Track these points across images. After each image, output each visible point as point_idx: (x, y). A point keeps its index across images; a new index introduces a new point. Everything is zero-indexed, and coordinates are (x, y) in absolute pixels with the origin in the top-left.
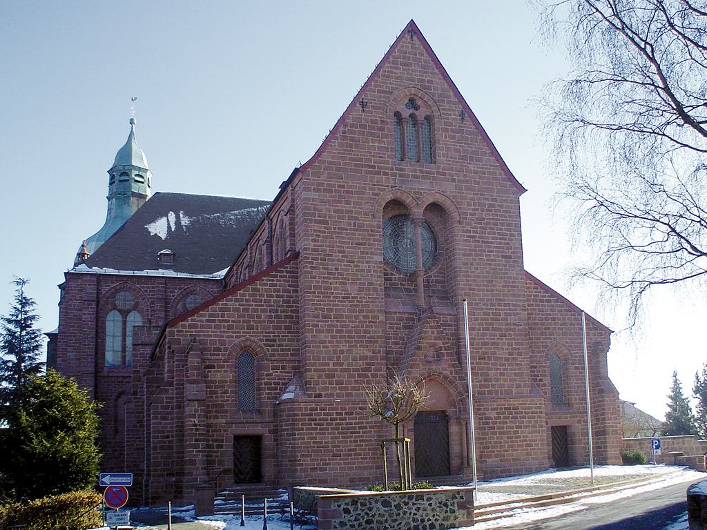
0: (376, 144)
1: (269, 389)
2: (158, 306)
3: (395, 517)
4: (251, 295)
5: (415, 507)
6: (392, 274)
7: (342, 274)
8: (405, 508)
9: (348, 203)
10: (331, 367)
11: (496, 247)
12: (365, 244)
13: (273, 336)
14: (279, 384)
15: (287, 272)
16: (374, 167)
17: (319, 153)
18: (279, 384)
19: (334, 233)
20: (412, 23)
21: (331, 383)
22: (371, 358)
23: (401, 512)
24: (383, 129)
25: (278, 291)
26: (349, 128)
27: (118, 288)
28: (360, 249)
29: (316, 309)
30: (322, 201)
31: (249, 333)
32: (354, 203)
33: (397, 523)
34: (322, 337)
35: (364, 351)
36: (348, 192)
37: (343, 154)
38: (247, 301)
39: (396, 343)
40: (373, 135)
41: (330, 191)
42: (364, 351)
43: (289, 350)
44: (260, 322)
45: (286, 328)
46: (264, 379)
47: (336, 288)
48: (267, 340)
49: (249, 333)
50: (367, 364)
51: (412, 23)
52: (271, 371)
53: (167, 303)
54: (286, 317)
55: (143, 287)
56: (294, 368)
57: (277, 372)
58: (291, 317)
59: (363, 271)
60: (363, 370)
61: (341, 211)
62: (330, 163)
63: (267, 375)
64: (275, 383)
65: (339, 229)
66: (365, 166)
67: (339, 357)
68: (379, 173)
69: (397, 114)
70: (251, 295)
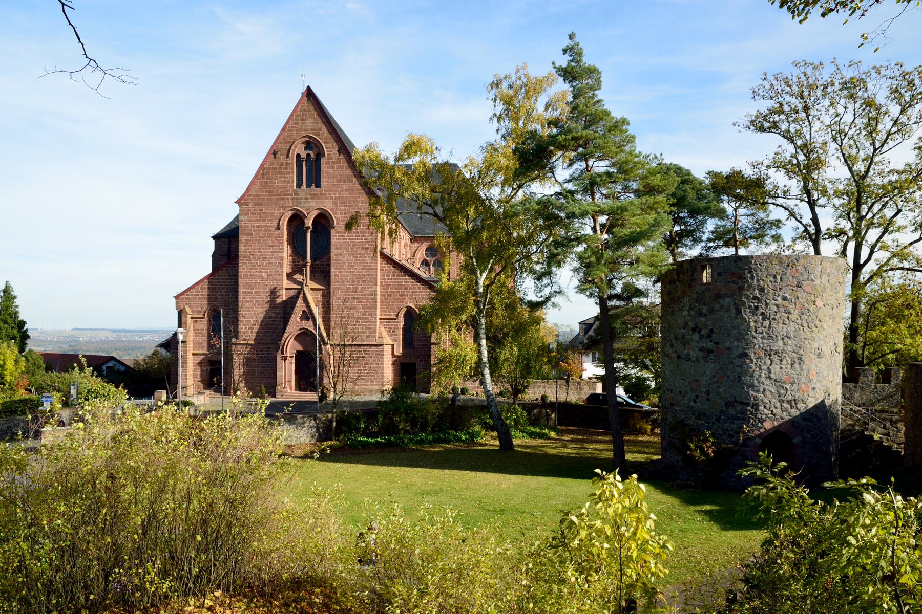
7: (259, 266)
9: (264, 220)
16: (280, 195)
17: (248, 189)
20: (309, 88)
22: (275, 317)
24: (286, 168)
25: (231, 276)
30: (250, 221)
36: (264, 213)
40: (280, 173)
41: (255, 214)
47: (256, 275)
51: (309, 88)
60: (270, 325)
61: (260, 226)
62: (254, 196)
68: (283, 199)
69: (298, 155)
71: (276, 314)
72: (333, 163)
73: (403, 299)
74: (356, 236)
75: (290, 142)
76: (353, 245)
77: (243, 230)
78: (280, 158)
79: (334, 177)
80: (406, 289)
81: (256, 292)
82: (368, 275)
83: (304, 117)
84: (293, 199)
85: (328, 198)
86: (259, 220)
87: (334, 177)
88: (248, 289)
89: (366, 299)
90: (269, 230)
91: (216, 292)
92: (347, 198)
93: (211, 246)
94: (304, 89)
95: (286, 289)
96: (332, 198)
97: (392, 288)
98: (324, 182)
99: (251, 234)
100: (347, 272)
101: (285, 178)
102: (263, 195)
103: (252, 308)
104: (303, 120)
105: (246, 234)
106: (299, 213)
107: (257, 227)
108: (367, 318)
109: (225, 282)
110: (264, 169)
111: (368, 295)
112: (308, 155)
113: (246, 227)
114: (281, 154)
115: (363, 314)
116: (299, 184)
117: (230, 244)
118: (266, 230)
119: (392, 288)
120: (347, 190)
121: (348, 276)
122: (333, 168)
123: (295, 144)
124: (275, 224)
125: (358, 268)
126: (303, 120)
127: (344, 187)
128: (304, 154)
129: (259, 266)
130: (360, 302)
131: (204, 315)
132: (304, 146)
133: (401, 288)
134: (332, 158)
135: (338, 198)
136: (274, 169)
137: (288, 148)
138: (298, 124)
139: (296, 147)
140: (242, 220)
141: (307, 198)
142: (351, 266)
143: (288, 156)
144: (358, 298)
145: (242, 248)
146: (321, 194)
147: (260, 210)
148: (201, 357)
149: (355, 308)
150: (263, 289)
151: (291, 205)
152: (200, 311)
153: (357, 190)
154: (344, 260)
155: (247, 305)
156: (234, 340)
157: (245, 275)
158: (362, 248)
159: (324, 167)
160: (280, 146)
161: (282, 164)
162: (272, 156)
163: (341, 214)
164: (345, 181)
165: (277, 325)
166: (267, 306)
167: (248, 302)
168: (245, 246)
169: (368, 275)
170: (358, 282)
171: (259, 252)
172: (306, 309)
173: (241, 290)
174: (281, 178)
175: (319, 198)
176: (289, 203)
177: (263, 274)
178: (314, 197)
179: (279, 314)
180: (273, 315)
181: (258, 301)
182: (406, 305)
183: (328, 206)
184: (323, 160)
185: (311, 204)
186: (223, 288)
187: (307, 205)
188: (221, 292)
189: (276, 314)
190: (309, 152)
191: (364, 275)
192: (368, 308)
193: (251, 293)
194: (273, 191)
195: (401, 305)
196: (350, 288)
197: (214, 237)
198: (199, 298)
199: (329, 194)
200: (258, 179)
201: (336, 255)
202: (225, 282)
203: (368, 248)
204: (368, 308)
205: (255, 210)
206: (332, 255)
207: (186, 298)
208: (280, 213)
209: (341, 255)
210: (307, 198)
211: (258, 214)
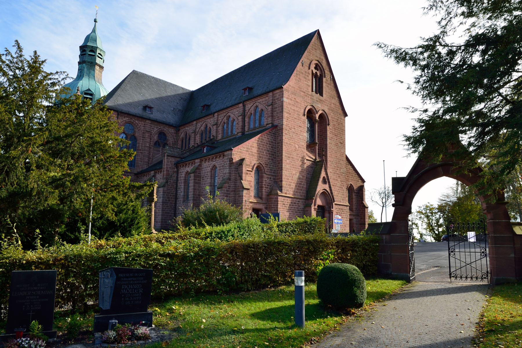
1: (266, 187)
2: (147, 135)
9: (297, 107)
19: (292, 119)
21: (290, 188)
22: (302, 179)
27: (127, 121)
47: (292, 145)
52: (266, 179)
53: (151, 135)
55: (139, 123)
56: (274, 179)
66: (302, 92)
71: (303, 176)
73: (349, 179)
75: (310, 60)
89: (342, 175)
95: (307, 160)
96: (328, 106)
98: (324, 95)
103: (290, 169)
105: (287, 113)
106: (313, 109)
108: (342, 188)
113: (287, 107)
128: (314, 71)
141: (317, 101)
149: (337, 180)
151: (310, 102)
159: (324, 84)
161: (306, 72)
172: (325, 176)
174: (305, 81)
180: (301, 177)
182: (350, 183)
184: (324, 79)
186: (265, 150)
188: (263, 152)
198: (249, 154)
205: (292, 97)
208: (305, 105)
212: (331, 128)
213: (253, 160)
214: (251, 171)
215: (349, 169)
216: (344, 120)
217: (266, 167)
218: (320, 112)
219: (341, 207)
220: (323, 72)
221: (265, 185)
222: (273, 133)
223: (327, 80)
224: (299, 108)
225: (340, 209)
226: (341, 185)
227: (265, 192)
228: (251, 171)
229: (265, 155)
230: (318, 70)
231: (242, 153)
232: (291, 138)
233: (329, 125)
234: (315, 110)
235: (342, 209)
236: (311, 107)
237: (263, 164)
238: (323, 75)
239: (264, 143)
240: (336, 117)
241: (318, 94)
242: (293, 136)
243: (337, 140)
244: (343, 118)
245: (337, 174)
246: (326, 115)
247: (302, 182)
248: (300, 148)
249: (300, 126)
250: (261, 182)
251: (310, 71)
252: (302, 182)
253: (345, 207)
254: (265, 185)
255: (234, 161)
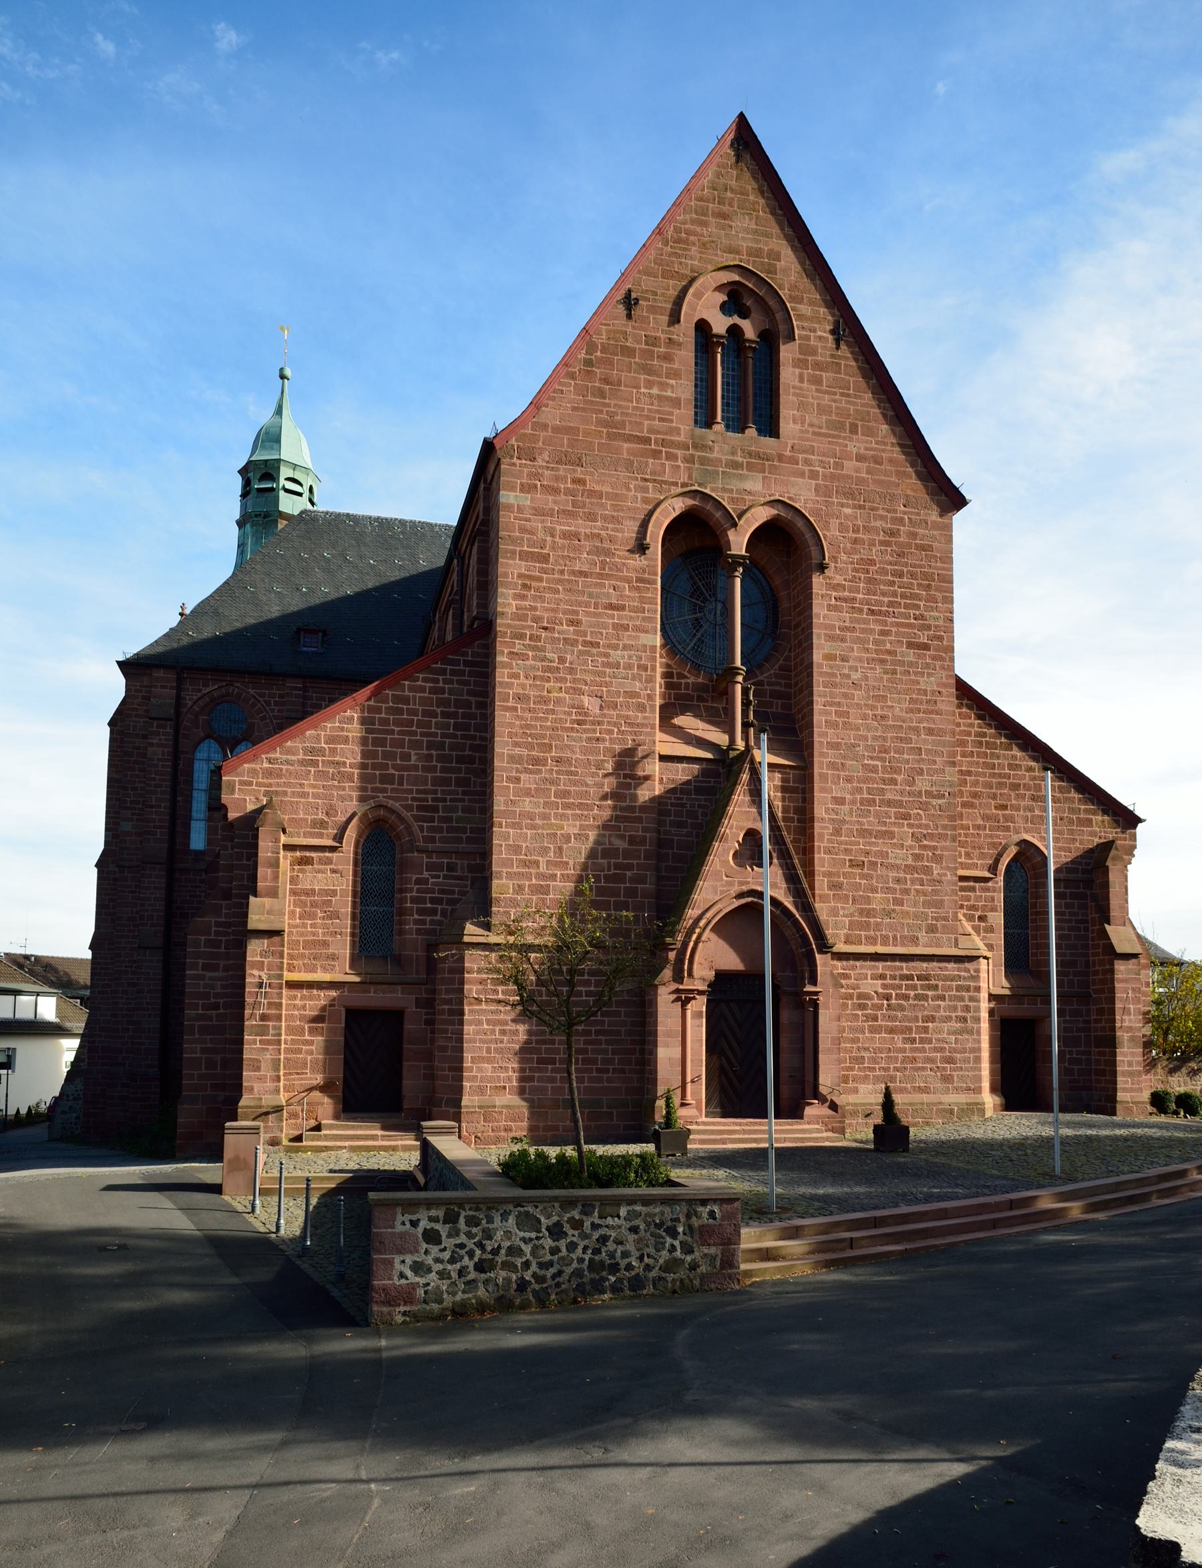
0: (655, 391)
1: (421, 912)
3: (548, 1257)
4: (391, 711)
5: (596, 1235)
6: (681, 676)
8: (572, 1234)
9: (591, 517)
10: (543, 868)
11: (898, 625)
12: (623, 608)
13: (434, 800)
14: (439, 901)
15: (466, 663)
16: (647, 441)
17: (536, 405)
18: (439, 901)
19: (560, 581)
20: (742, 122)
22: (627, 854)
23: (562, 1244)
24: (667, 358)
26: (599, 354)
28: (613, 617)
29: (516, 744)
31: (385, 790)
32: (605, 518)
33: (552, 1271)
34: (527, 804)
35: (613, 839)
36: (592, 493)
37: (583, 409)
38: (384, 722)
39: (680, 825)
40: (648, 370)
41: (556, 491)
42: (613, 839)
43: (464, 830)
44: (407, 768)
45: (459, 782)
46: (411, 890)
47: (558, 701)
48: (419, 808)
49: (385, 790)
50: (617, 866)
52: (426, 874)
54: (460, 760)
56: (471, 869)
57: (438, 877)
58: (471, 760)
59: (617, 666)
61: (576, 536)
62: (556, 430)
63: (418, 882)
64: (433, 901)
65: (573, 573)
66: (630, 438)
67: (560, 849)
68: (656, 454)
69: (702, 327)
70: (391, 711)
71: (632, 841)
72: (818, 366)
73: (1008, 819)
74: (891, 604)
76: (882, 633)
77: (513, 541)
78: (645, 320)
79: (822, 410)
80: (1015, 787)
81: (558, 761)
82: (930, 732)
83: (726, 208)
84: (689, 460)
85: (802, 475)
86: (571, 514)
87: (822, 410)
88: (531, 747)
89: (924, 806)
90: (608, 553)
91: (386, 755)
92: (861, 481)
93: (115, 688)
94: (725, 123)
95: (663, 758)
96: (814, 475)
97: (976, 783)
98: (788, 424)
99: (545, 559)
100: (865, 717)
101: (663, 386)
102: (587, 433)
103: (545, 817)
104: (724, 216)
105: (524, 556)
106: (709, 507)
107: (564, 535)
108: (927, 870)
109: (420, 724)
110: (591, 348)
111: (929, 794)
112: (734, 331)
113: (523, 530)
114: (653, 309)
115: (917, 857)
116: (705, 419)
117: (179, 689)
118: (597, 551)
119: (976, 783)
120: (860, 458)
121: (868, 728)
122: (817, 381)
123: (696, 285)
124: (630, 530)
125: (898, 707)
126: (724, 216)
127: (855, 446)
128: (720, 324)
129: (571, 671)
130: (906, 817)
131: (339, 837)
132: (722, 297)
133: (1000, 785)
134: (814, 352)
135: (833, 477)
136: (628, 352)
137: (673, 293)
138: (704, 224)
139: (698, 295)
140: (509, 507)
141: (735, 465)
142: (877, 698)
143: (675, 318)
144: (899, 804)
145: (507, 602)
146: (781, 458)
147: (574, 481)
148: (323, 998)
149: (891, 835)
150: (585, 751)
151: (684, 478)
152: (323, 824)
153: (891, 461)
154: (855, 676)
155: (527, 804)
156: (472, 931)
157: (519, 698)
158: (910, 645)
159: (788, 375)
160: (647, 283)
161: (652, 341)
162: (621, 310)
163: (842, 528)
164: (854, 429)
165: (632, 880)
166: (604, 811)
167: (528, 793)
168: (523, 597)
169: (930, 732)
170: (900, 751)
171: (571, 623)
173: (503, 748)
174: (649, 384)
175: (773, 469)
176: (678, 472)
177: (586, 700)
178: (758, 462)
179: (643, 841)
180: (621, 845)
181: (565, 794)
182: (1016, 838)
183: (803, 495)
184: (787, 352)
185: (749, 485)
186: (415, 745)
187: (735, 484)
188: (406, 757)
189: (632, 841)
190: (736, 319)
191: (916, 730)
192: (931, 836)
193: (537, 761)
194: (622, 425)
195: (1001, 838)
196: (874, 769)
197: (124, 666)
198: (321, 775)
199: (807, 462)
200: (572, 376)
201: (829, 657)
202: (420, 724)
203: (926, 647)
204: (931, 836)
205: (557, 478)
206: (817, 657)
207: (269, 773)
208: (646, 501)
209: (844, 659)
210: (735, 465)
211: (568, 492)
212: (839, 579)
213: (343, 799)
214: (332, 849)
215: (1018, 767)
216: (948, 528)
217: (418, 819)
218: (761, 515)
219: (905, 968)
220: (779, 316)
221: (413, 900)
222: (466, 663)
223: (807, 350)
224: (605, 518)
225: (910, 978)
226: (917, 857)
227: (419, 932)
228: (332, 849)
229: (416, 768)
230: (744, 315)
231: (279, 776)
232: (549, 669)
233: (822, 568)
234: (718, 515)
235: (927, 978)
236: (690, 502)
237: (409, 808)
238: (782, 327)
239: (413, 712)
240: (878, 524)
241: (752, 432)
242: (562, 660)
243: (883, 633)
244: (934, 516)
245: (890, 803)
246: (800, 523)
247: (629, 867)
248: (615, 706)
249: (611, 607)
250: (401, 891)
251: (685, 332)
252: (629, 867)
253: (951, 965)
254: (413, 900)
255: (232, 815)
